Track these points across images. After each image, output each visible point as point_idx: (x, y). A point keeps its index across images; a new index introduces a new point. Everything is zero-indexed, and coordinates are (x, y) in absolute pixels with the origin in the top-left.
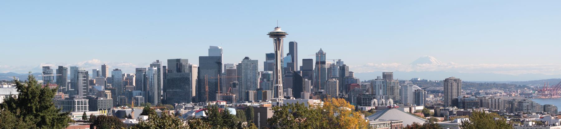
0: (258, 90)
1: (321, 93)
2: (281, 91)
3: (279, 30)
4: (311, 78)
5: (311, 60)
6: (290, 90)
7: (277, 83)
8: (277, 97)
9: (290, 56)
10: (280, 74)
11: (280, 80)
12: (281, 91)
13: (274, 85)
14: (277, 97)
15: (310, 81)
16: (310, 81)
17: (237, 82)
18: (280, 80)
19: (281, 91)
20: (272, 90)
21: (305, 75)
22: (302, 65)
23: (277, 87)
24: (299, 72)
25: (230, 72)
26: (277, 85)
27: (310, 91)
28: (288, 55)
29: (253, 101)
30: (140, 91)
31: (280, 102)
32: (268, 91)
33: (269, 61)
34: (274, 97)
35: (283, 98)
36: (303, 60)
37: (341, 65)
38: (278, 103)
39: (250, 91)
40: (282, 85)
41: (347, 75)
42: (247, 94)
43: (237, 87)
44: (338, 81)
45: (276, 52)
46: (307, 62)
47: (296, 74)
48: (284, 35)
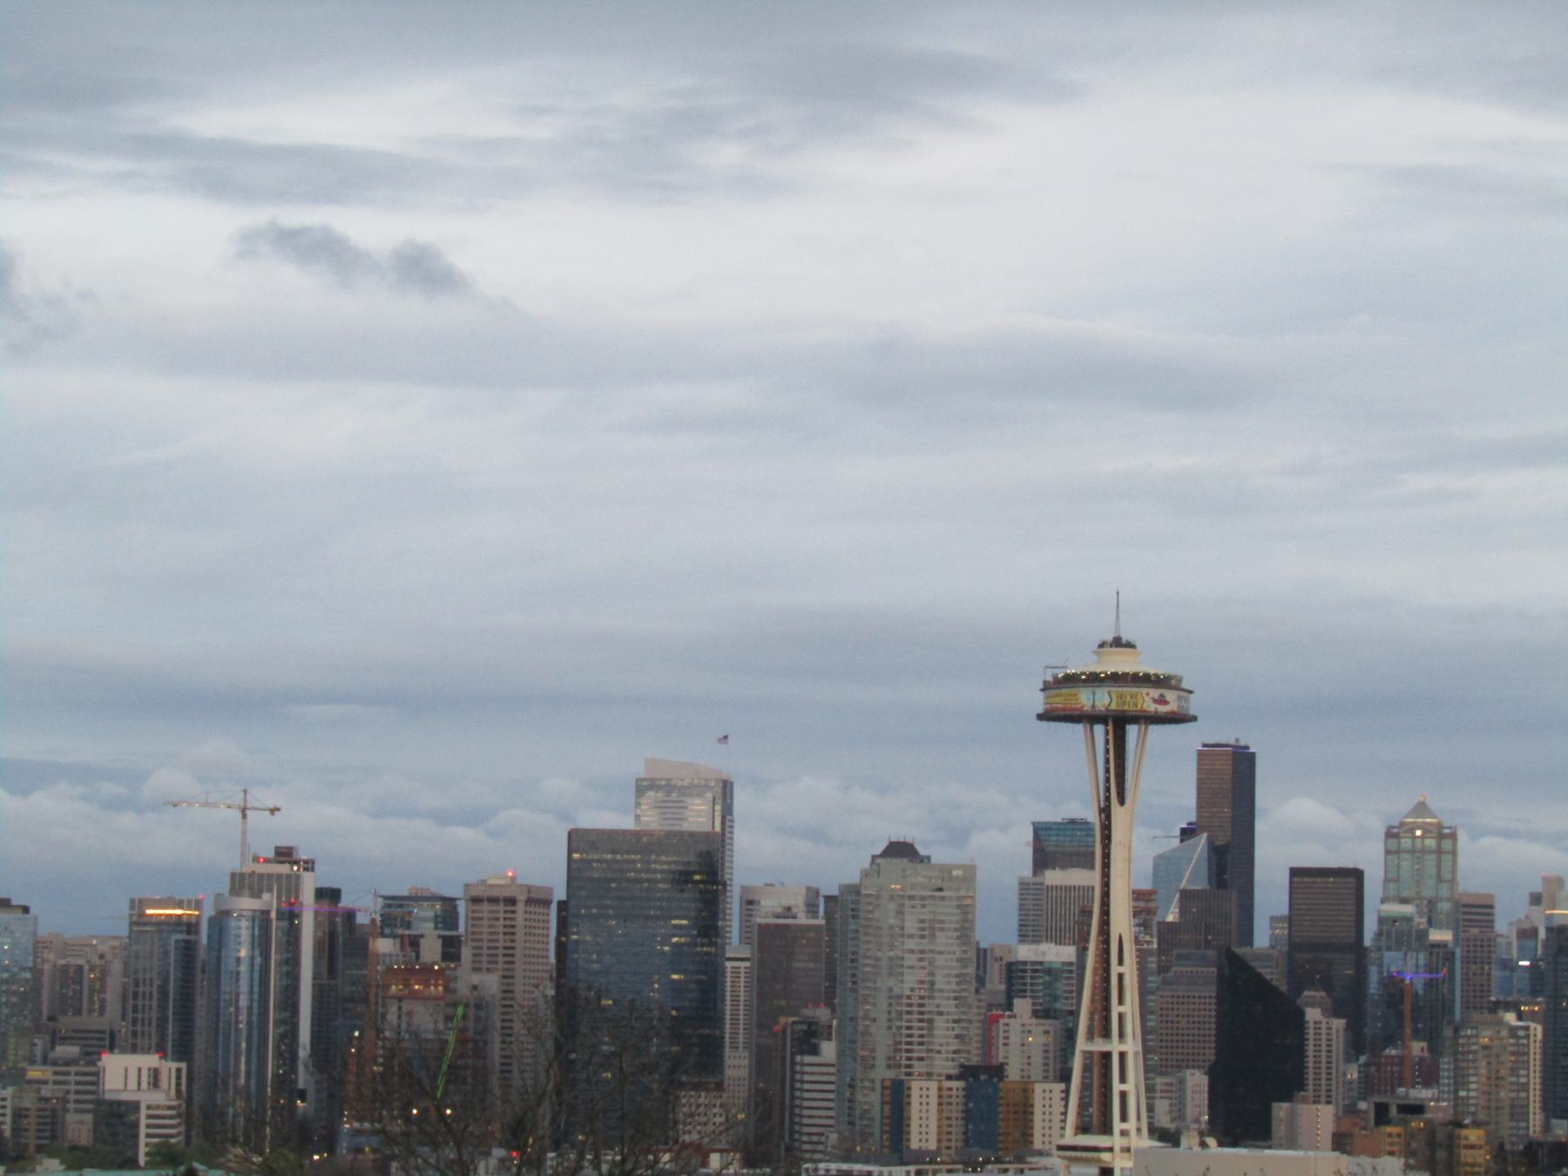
0: (967, 1073)
1: (1417, 1109)
2: (1129, 1087)
4: (1349, 1004)
5: (1357, 875)
6: (1197, 1082)
7: (1106, 1034)
8: (1106, 1129)
10: (1127, 970)
11: (1127, 1008)
13: (1081, 1044)
14: (1106, 1129)
15: (1339, 1023)
16: (1339, 1023)
17: (822, 1014)
18: (1127, 1008)
19: (1130, 1085)
22: (1284, 910)
23: (1107, 1056)
24: (1264, 957)
25: (775, 941)
26: (1099, 1046)
28: (1187, 833)
30: (153, 1060)
33: (1054, 877)
34: (1083, 1129)
36: (1295, 872)
39: (915, 1086)
40: (1132, 1046)
42: (897, 1096)
43: (829, 1050)
44: (1537, 1030)
45: (1106, 811)
46: (1327, 889)
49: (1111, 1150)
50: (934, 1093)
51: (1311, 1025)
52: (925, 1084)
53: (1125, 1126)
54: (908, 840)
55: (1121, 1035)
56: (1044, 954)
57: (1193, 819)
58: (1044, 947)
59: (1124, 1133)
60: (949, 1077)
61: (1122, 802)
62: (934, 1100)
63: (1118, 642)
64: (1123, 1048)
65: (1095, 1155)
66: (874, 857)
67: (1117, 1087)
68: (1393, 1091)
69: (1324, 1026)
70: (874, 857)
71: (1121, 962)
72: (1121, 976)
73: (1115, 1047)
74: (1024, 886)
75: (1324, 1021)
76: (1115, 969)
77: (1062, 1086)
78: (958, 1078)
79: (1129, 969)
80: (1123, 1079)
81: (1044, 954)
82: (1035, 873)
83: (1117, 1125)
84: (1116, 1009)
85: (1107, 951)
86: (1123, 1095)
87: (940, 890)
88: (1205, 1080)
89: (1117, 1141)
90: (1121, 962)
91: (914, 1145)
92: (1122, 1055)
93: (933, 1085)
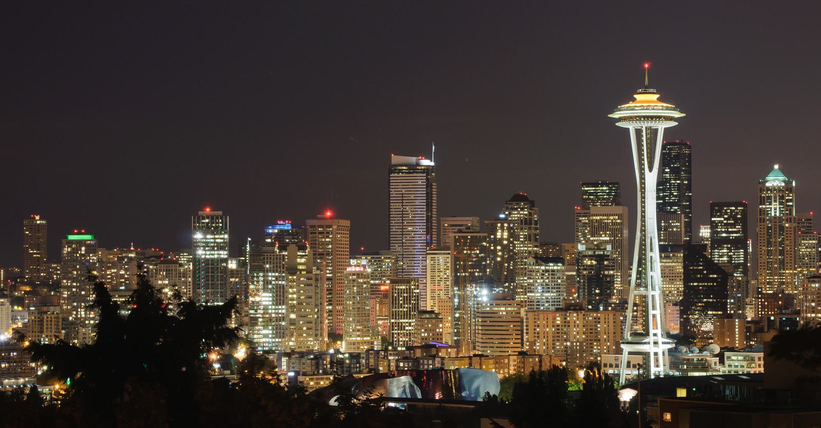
7: (646, 287)
8: (647, 334)
12: (657, 312)
19: (656, 312)
23: (645, 297)
38: (646, 355)
49: (649, 343)
53: (655, 331)
59: (655, 335)
61: (651, 169)
67: (651, 312)
71: (651, 250)
73: (651, 293)
76: (649, 254)
79: (655, 254)
80: (654, 308)
83: (652, 331)
85: (645, 245)
86: (654, 316)
89: (651, 339)
92: (653, 296)
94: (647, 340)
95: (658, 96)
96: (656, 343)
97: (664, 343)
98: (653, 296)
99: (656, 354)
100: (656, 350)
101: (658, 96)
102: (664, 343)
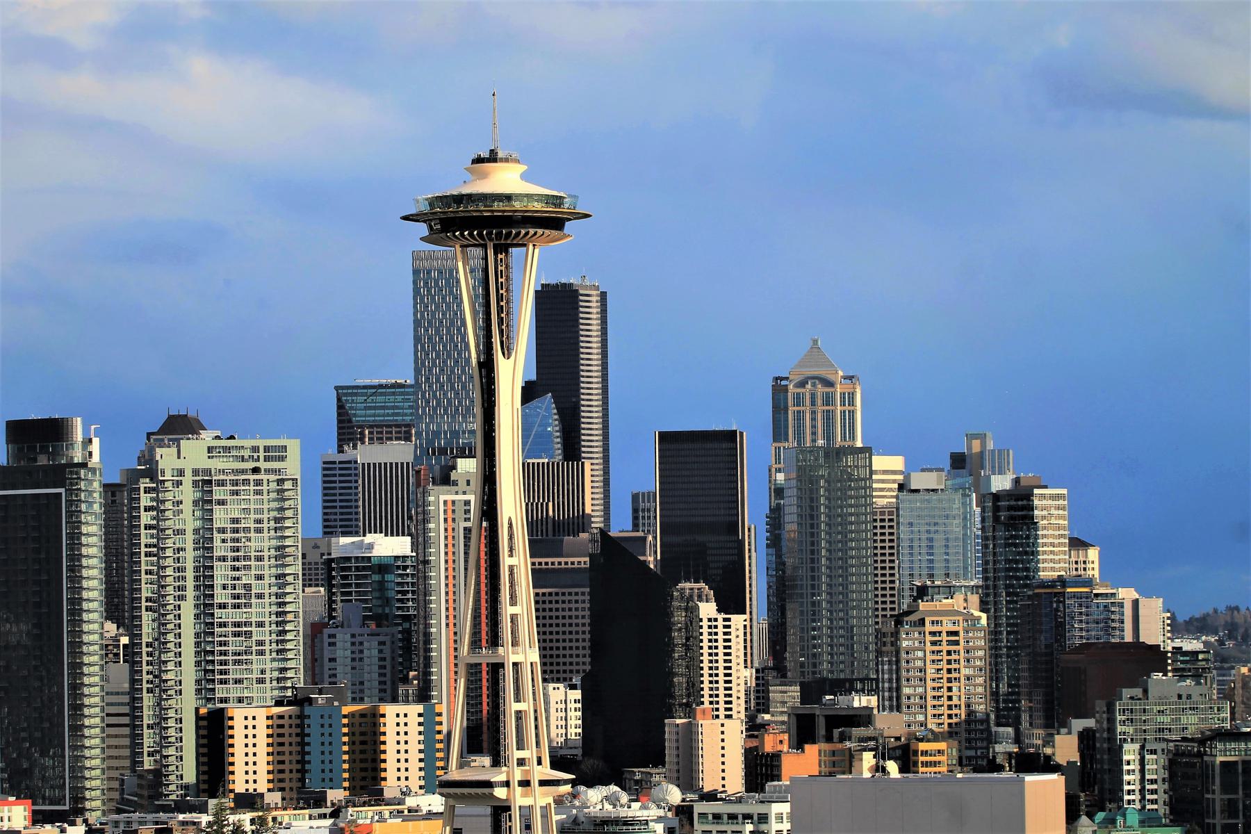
3: (506, 180)
7: (495, 641)
9: (546, 405)
16: (738, 620)
20: (424, 695)
21: (682, 561)
27: (739, 707)
29: (274, 798)
31: (520, 799)
32: (390, 710)
35: (547, 772)
36: (665, 437)
37: (1001, 483)
39: (238, 715)
41: (1053, 560)
42: (214, 731)
45: (487, 367)
46: (698, 459)
47: (615, 554)
48: (555, 223)
50: (262, 723)
51: (705, 623)
52: (250, 712)
54: (192, 414)
55: (515, 643)
56: (371, 547)
57: (534, 377)
58: (369, 538)
59: (521, 762)
60: (279, 703)
61: (507, 351)
62: (262, 732)
63: (493, 158)
64: (514, 658)
65: (486, 791)
66: (149, 435)
68: (818, 701)
69: (720, 623)
70: (149, 435)
72: (511, 568)
73: (510, 655)
74: (328, 466)
75: (721, 617)
77: (420, 708)
78: (290, 704)
79: (517, 561)
81: (371, 547)
82: (341, 451)
84: (507, 610)
87: (256, 470)
88: (577, 694)
90: (511, 550)
91: (240, 788)
93: (262, 714)
94: (502, 777)
95: (522, 168)
96: (525, 783)
97: (543, 783)
98: (515, 664)
99: (527, 813)
100: (527, 801)
101: (522, 168)
102: (543, 783)
